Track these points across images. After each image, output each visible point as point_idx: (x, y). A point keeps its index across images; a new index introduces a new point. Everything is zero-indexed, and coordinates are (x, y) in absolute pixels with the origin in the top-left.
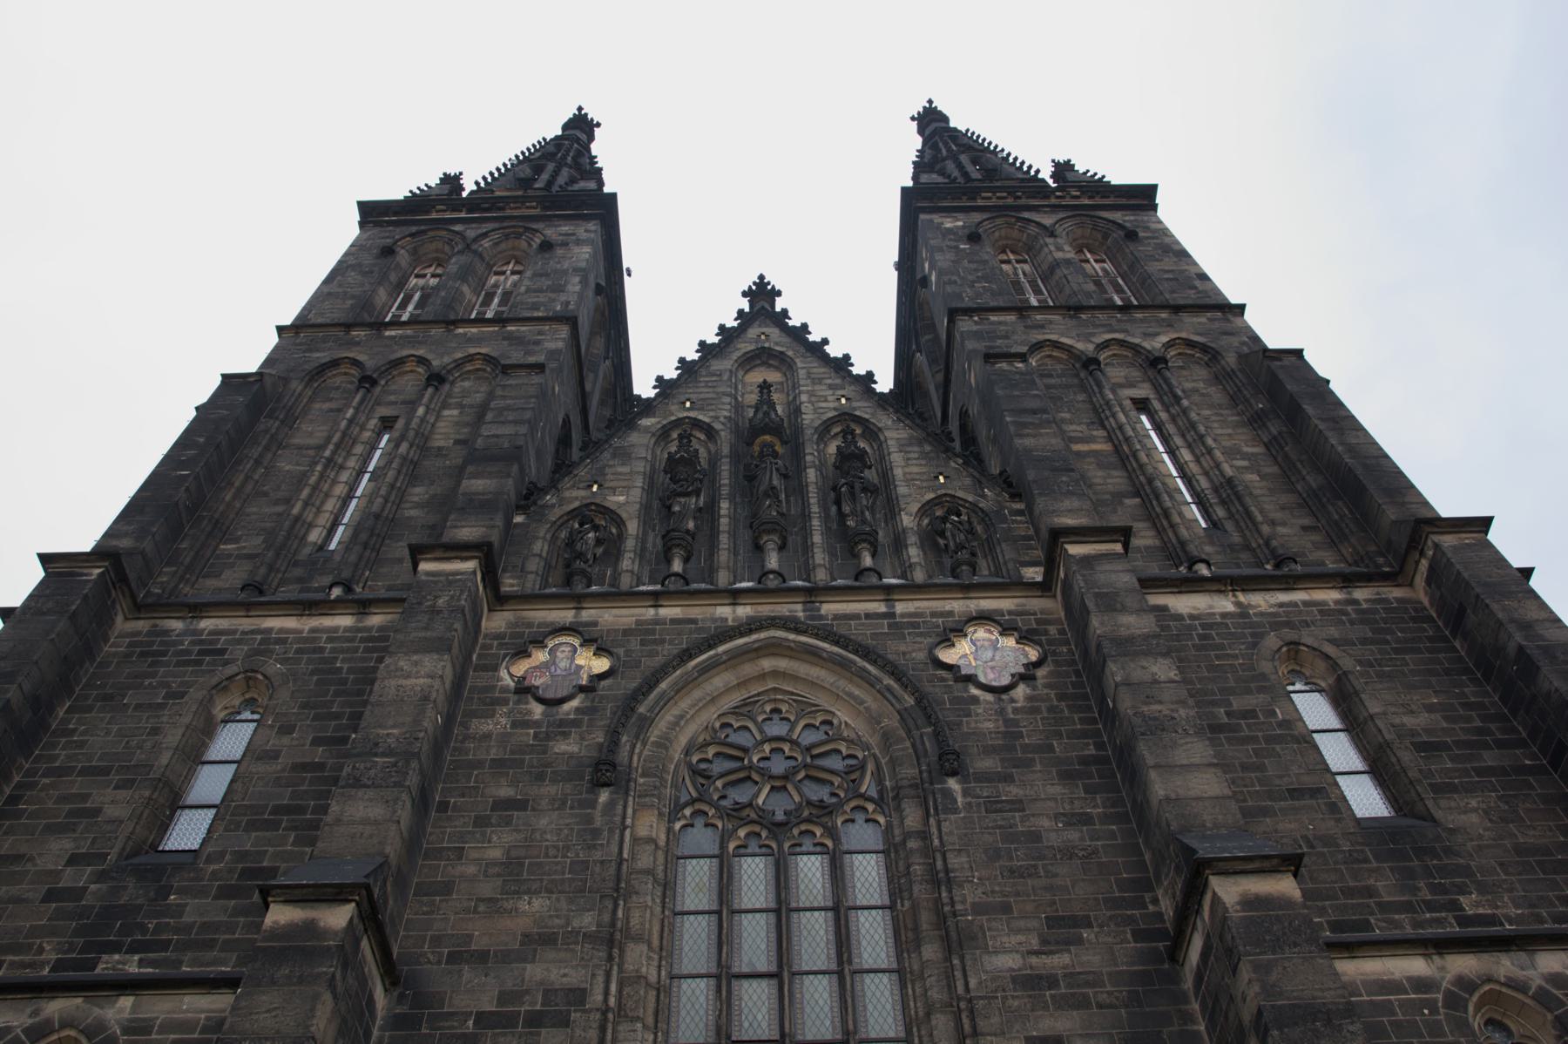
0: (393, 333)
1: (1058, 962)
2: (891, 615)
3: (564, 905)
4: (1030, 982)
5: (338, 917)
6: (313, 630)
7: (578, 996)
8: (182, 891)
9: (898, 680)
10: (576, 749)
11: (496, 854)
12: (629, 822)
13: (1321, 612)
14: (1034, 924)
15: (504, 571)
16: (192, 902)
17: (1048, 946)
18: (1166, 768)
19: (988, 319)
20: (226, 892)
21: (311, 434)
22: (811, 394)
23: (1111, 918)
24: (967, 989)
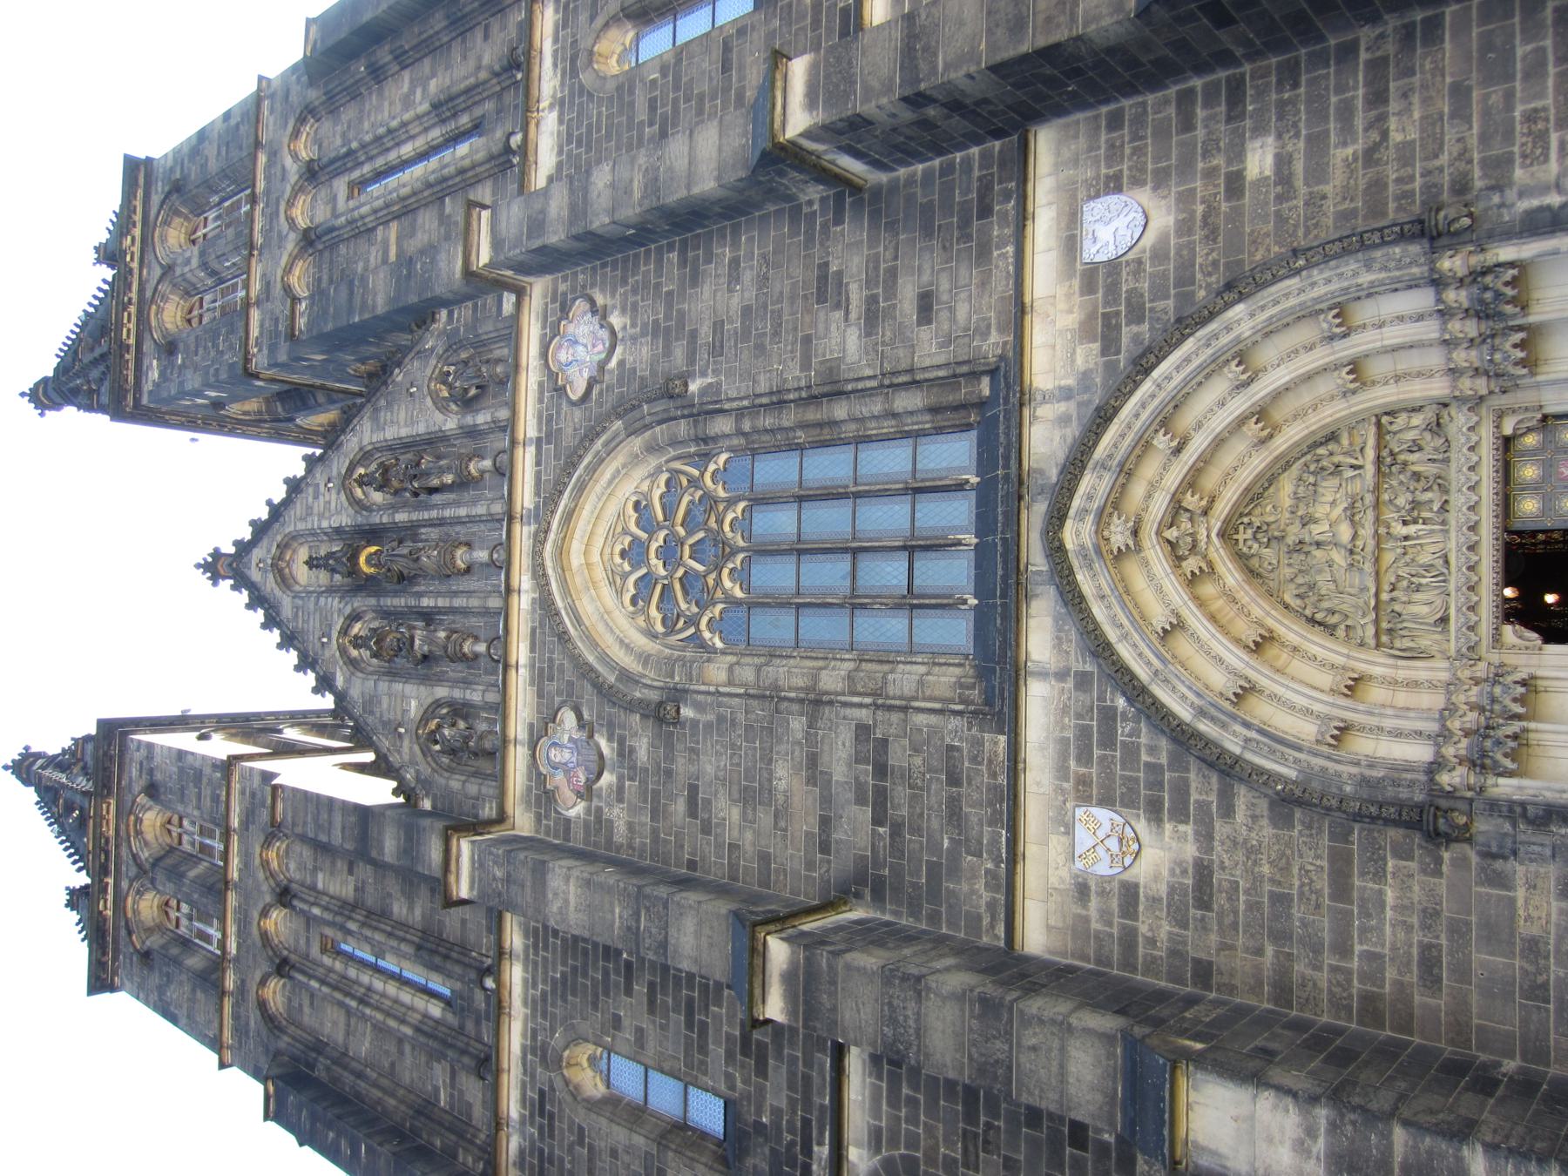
0: (234, 946)
1: (856, 295)
3: (783, 748)
4: (872, 317)
5: (778, 951)
6: (525, 1003)
7: (862, 731)
8: (759, 1112)
9: (598, 435)
10: (645, 740)
11: (735, 813)
12: (712, 689)
13: (564, 27)
14: (822, 315)
15: (476, 816)
16: (769, 1100)
17: (842, 304)
18: (690, 181)
20: (762, 1070)
21: (335, 1023)
22: (321, 516)
23: (822, 244)
24: (874, 377)
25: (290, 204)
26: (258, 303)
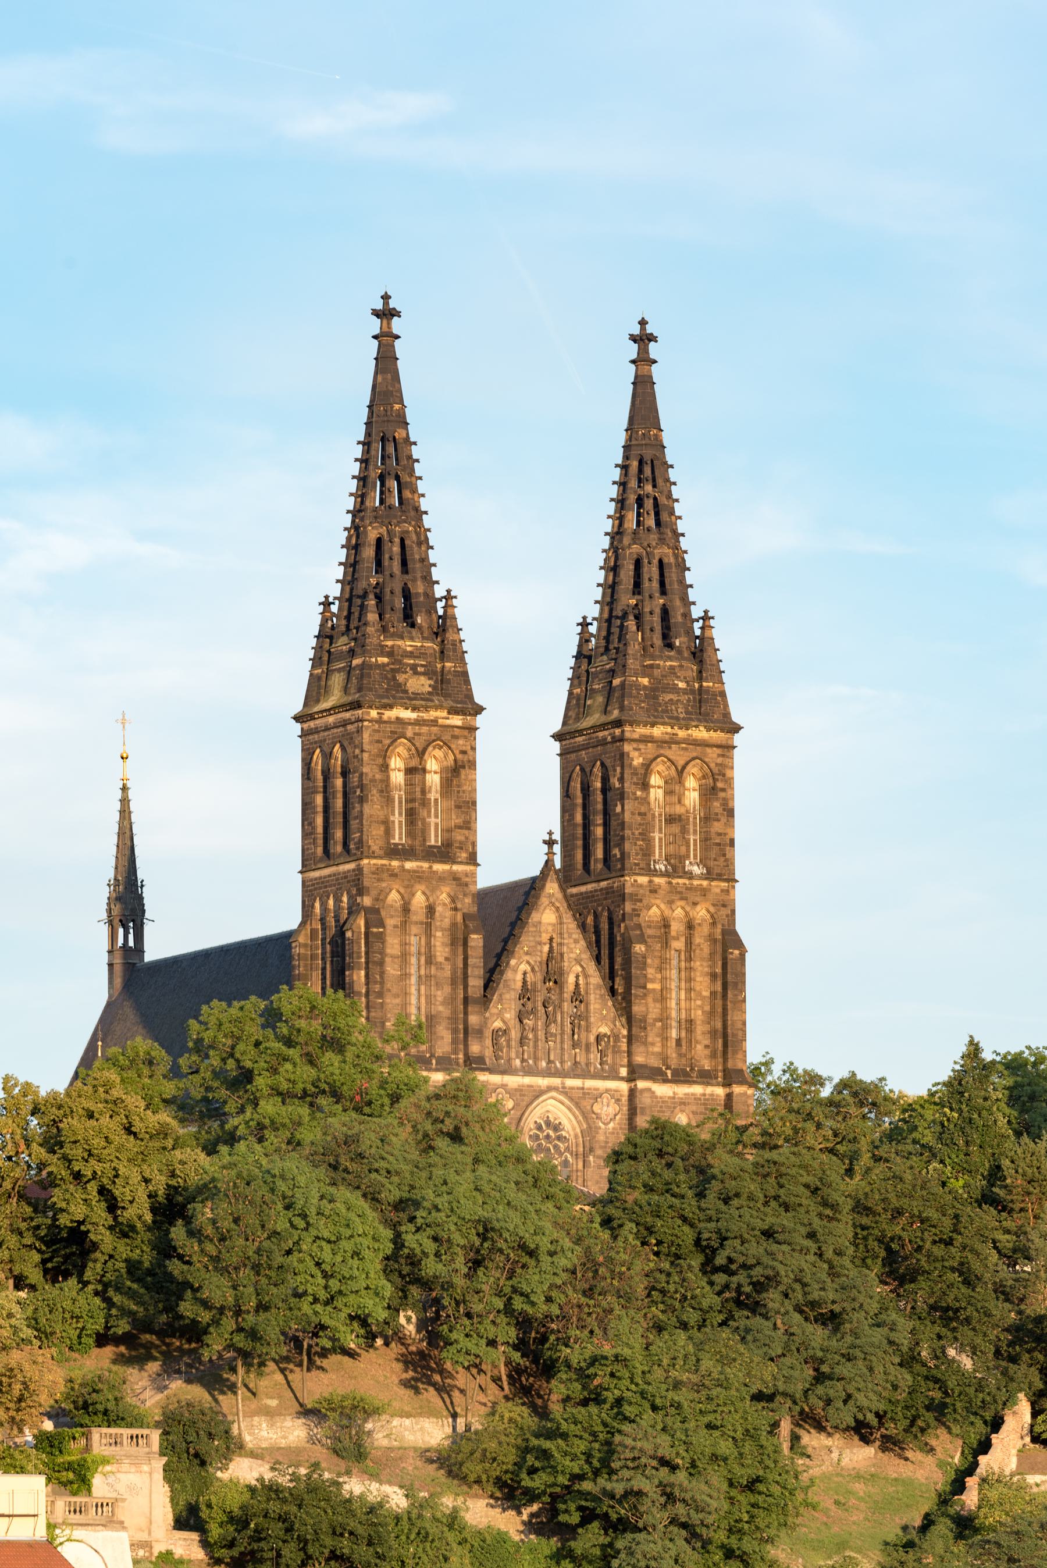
2: (583, 1088)
19: (635, 881)
25: (683, 908)
26: (650, 882)
